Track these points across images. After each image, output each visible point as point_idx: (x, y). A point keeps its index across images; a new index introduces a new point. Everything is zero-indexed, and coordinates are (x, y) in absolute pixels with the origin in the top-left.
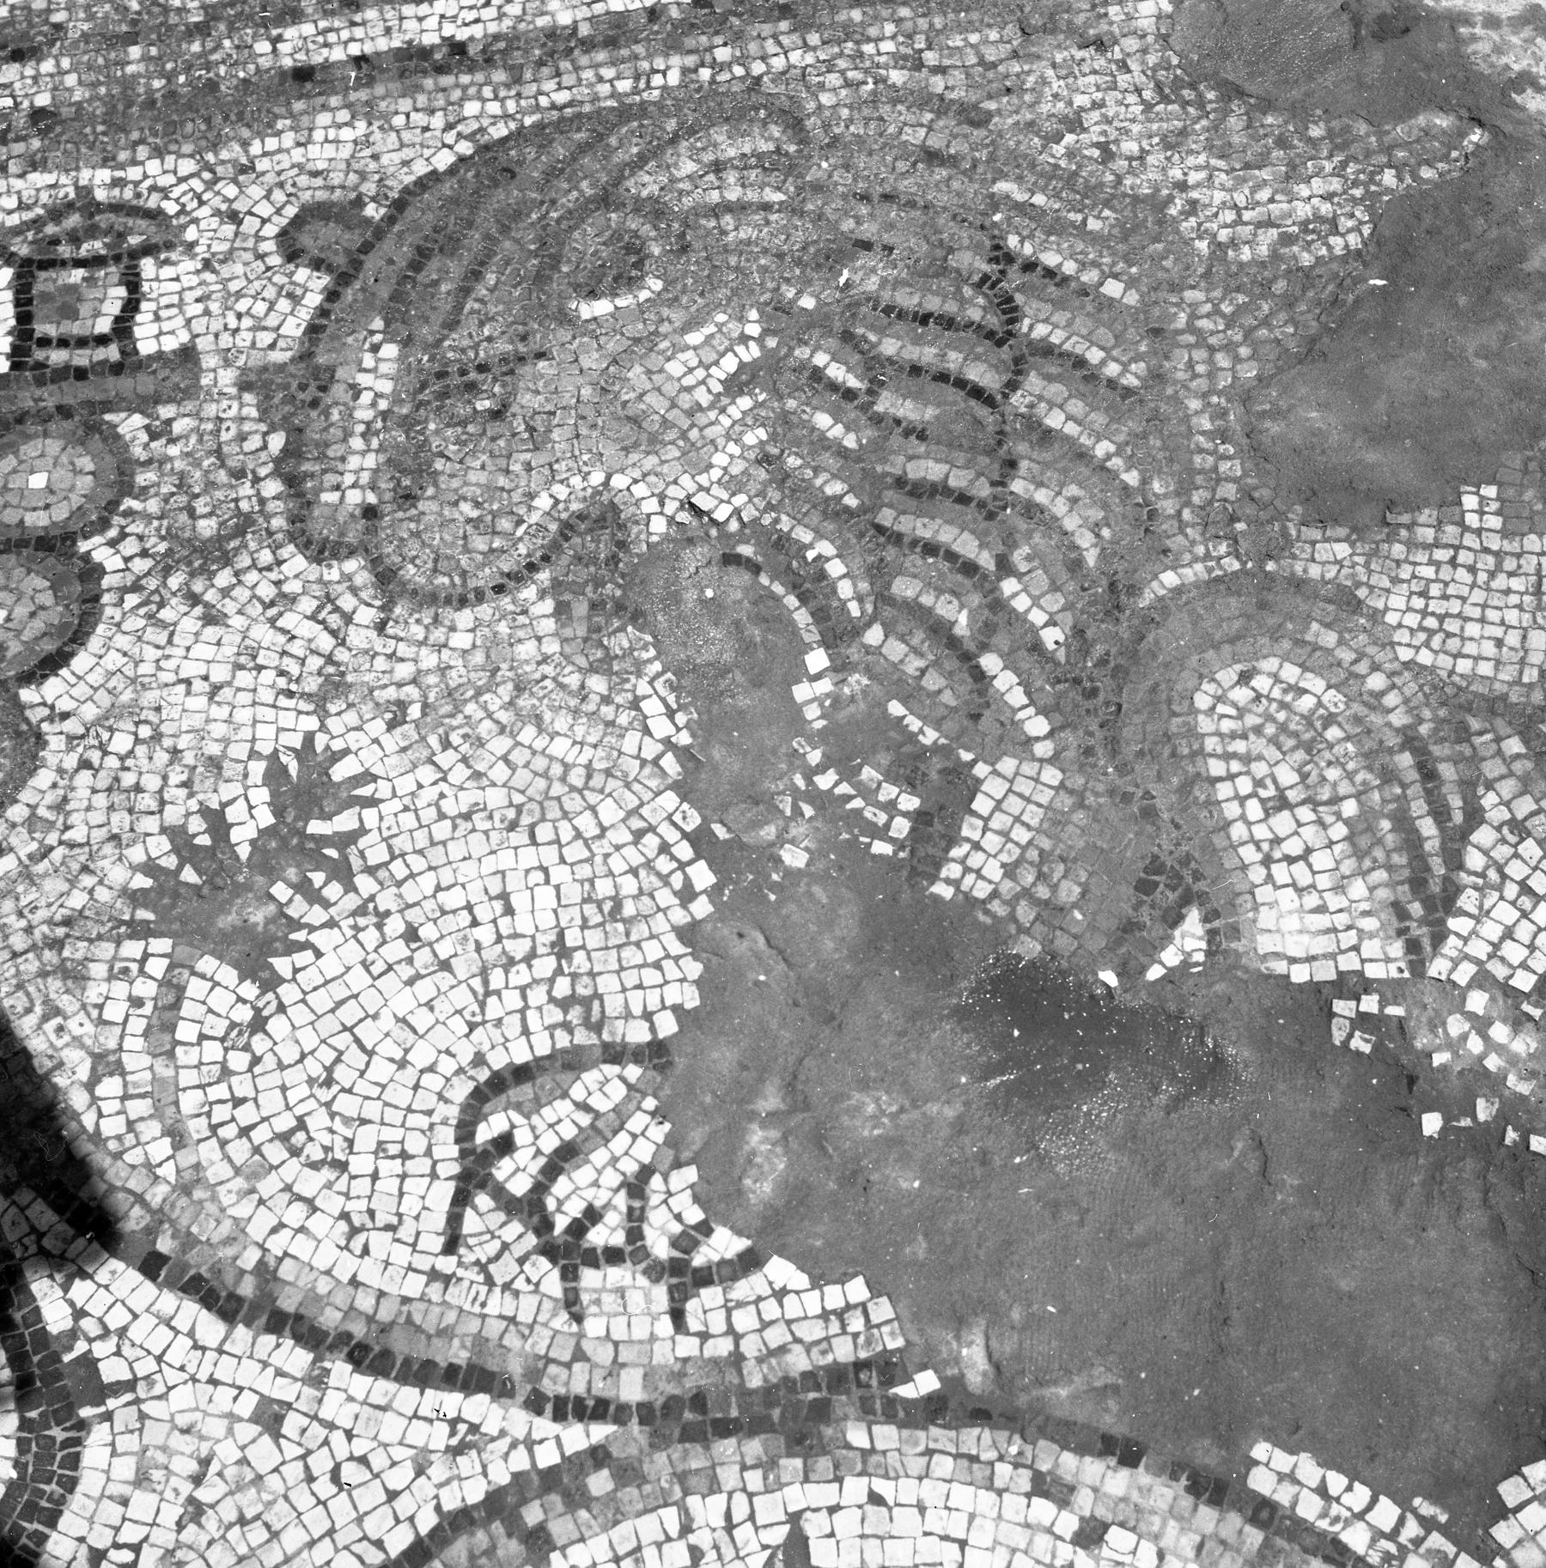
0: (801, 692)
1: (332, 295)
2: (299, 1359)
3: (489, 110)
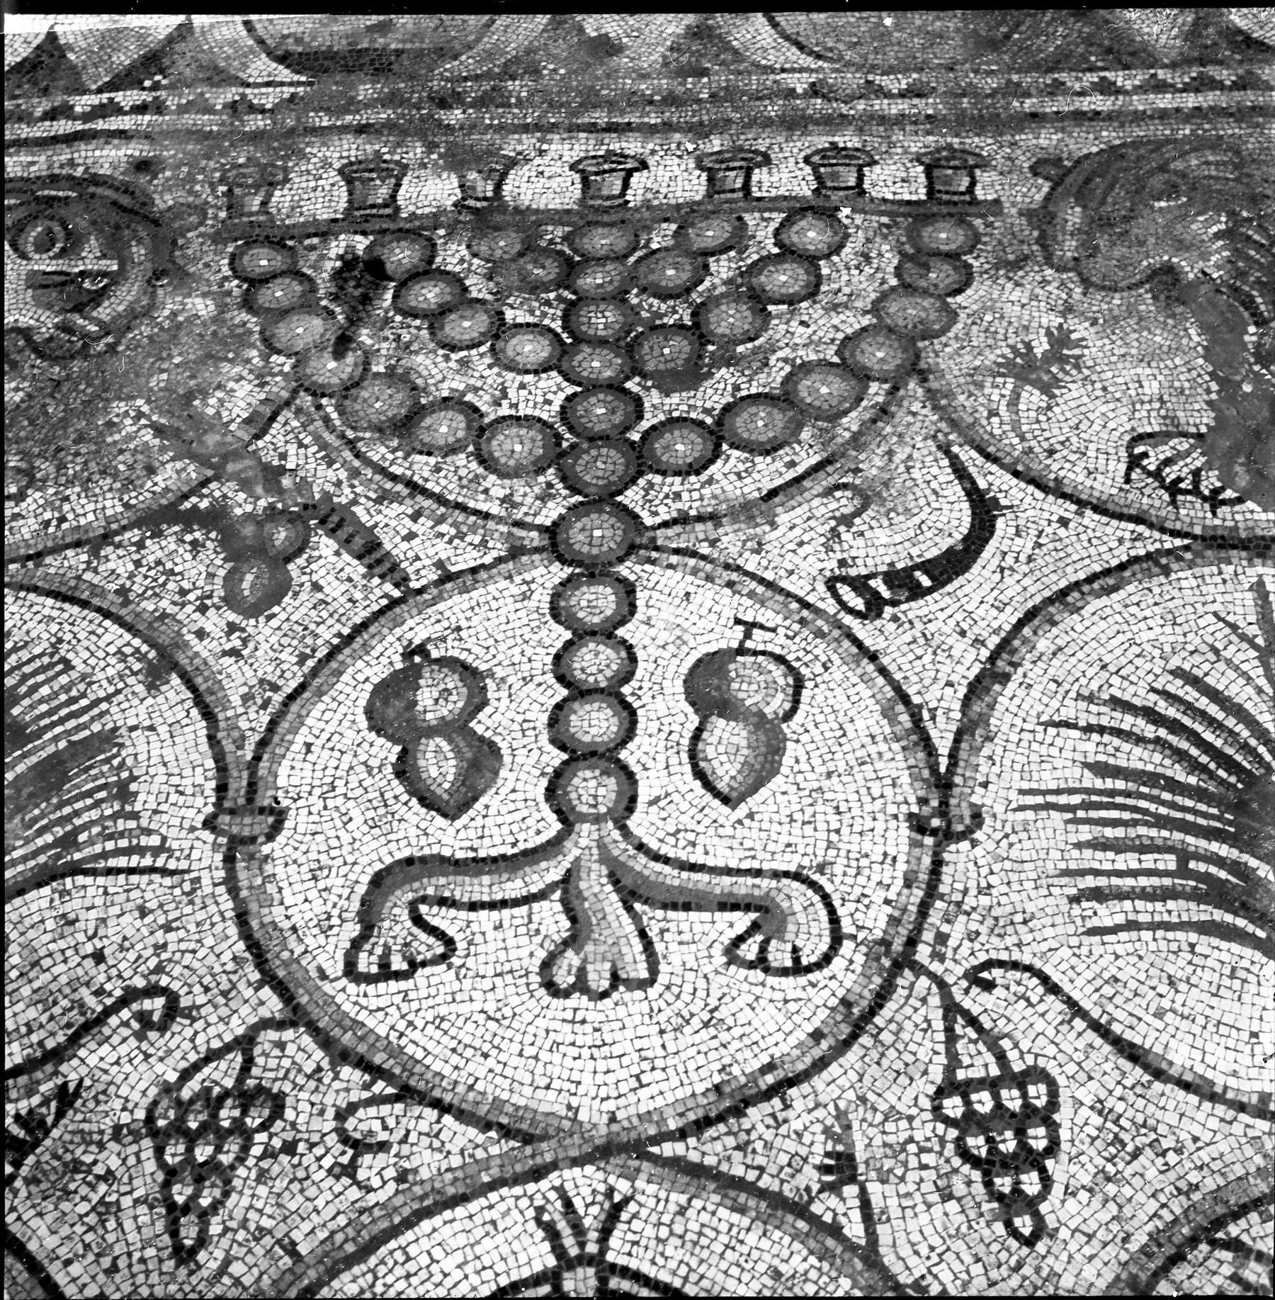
0: (1247, 338)
1: (1053, 189)
2: (1074, 507)
3: (1110, 135)
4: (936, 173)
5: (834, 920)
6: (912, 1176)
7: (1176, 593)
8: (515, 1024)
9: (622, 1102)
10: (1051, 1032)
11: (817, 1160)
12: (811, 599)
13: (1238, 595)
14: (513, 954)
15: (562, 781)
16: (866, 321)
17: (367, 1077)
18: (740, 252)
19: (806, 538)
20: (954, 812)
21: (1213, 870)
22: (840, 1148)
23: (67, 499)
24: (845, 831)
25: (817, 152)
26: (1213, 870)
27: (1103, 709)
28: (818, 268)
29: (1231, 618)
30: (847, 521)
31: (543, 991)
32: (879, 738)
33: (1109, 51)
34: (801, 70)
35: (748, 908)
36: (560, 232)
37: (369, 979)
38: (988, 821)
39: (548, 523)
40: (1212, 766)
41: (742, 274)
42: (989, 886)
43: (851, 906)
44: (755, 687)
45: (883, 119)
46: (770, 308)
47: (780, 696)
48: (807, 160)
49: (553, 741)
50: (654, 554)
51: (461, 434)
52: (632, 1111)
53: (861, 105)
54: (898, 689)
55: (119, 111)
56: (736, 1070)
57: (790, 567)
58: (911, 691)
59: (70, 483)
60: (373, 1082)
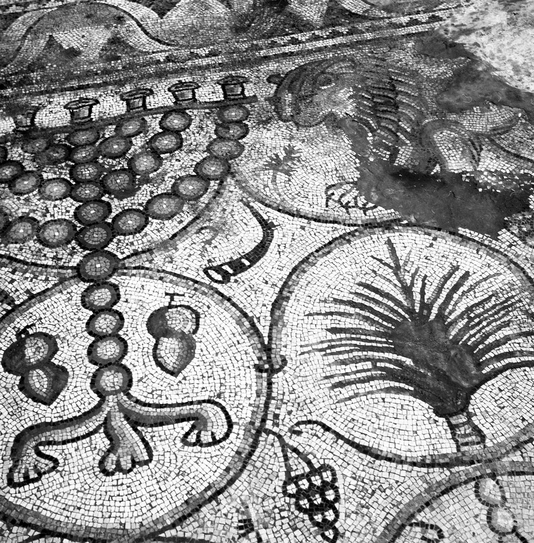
1: (278, 87)
2: (306, 221)
3: (300, 61)
4: (227, 87)
5: (228, 417)
6: (278, 523)
7: (354, 250)
8: (91, 492)
9: (144, 517)
10: (329, 448)
11: (235, 525)
12: (198, 279)
13: (380, 247)
14: (85, 460)
15: (97, 378)
16: (205, 155)
17: (25, 529)
18: (145, 134)
19: (192, 253)
20: (274, 361)
21: (388, 365)
22: (245, 517)
24: (227, 377)
25: (173, 86)
26: (388, 365)
27: (331, 305)
28: (181, 135)
29: (379, 257)
30: (209, 242)
31: (101, 474)
32: (237, 334)
33: (293, 26)
34: (161, 51)
35: (188, 420)
36: (63, 136)
37: (21, 485)
38: (289, 361)
39: (75, 265)
40: (380, 321)
41: (147, 143)
42: (294, 390)
43: (235, 410)
44: (178, 321)
45: (200, 68)
46: (162, 156)
47: (190, 323)
48: (169, 90)
49: (91, 361)
50: (125, 271)
51: (30, 232)
52: (150, 520)
53: (190, 63)
54: (241, 311)
56: (194, 492)
57: (186, 266)
58: (247, 311)
60: (28, 531)
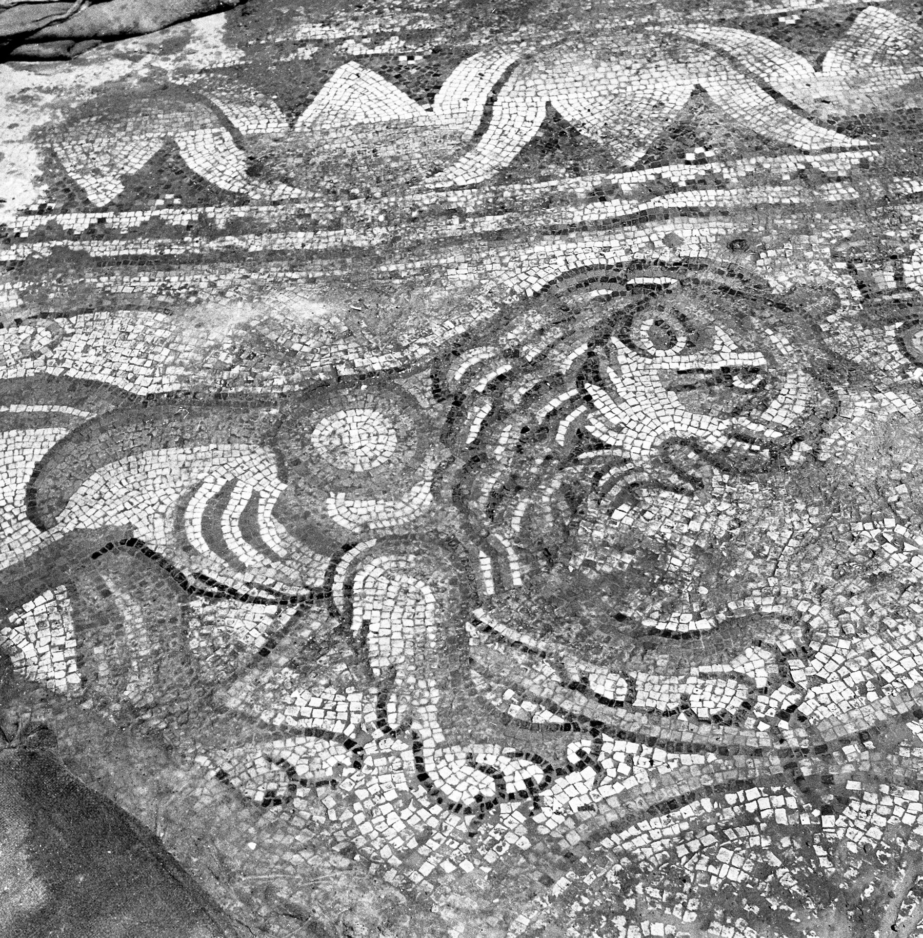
23: (871, 654)
55: (674, 188)
59: (862, 630)
